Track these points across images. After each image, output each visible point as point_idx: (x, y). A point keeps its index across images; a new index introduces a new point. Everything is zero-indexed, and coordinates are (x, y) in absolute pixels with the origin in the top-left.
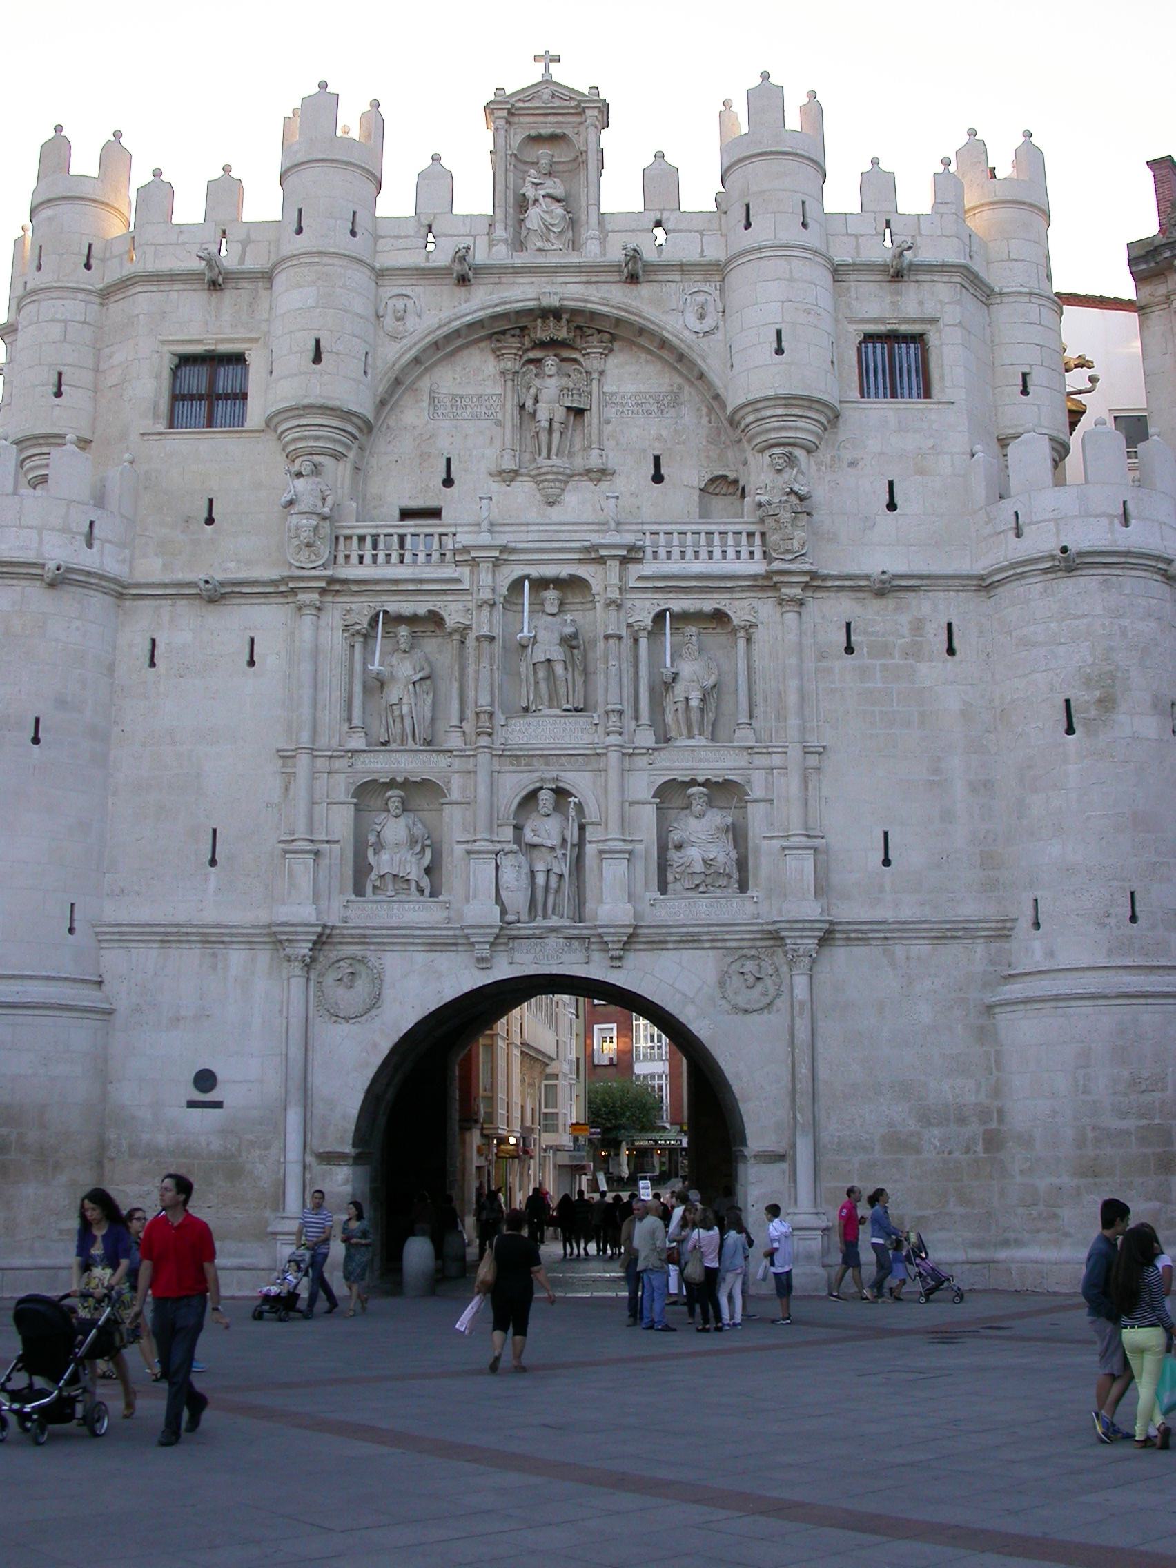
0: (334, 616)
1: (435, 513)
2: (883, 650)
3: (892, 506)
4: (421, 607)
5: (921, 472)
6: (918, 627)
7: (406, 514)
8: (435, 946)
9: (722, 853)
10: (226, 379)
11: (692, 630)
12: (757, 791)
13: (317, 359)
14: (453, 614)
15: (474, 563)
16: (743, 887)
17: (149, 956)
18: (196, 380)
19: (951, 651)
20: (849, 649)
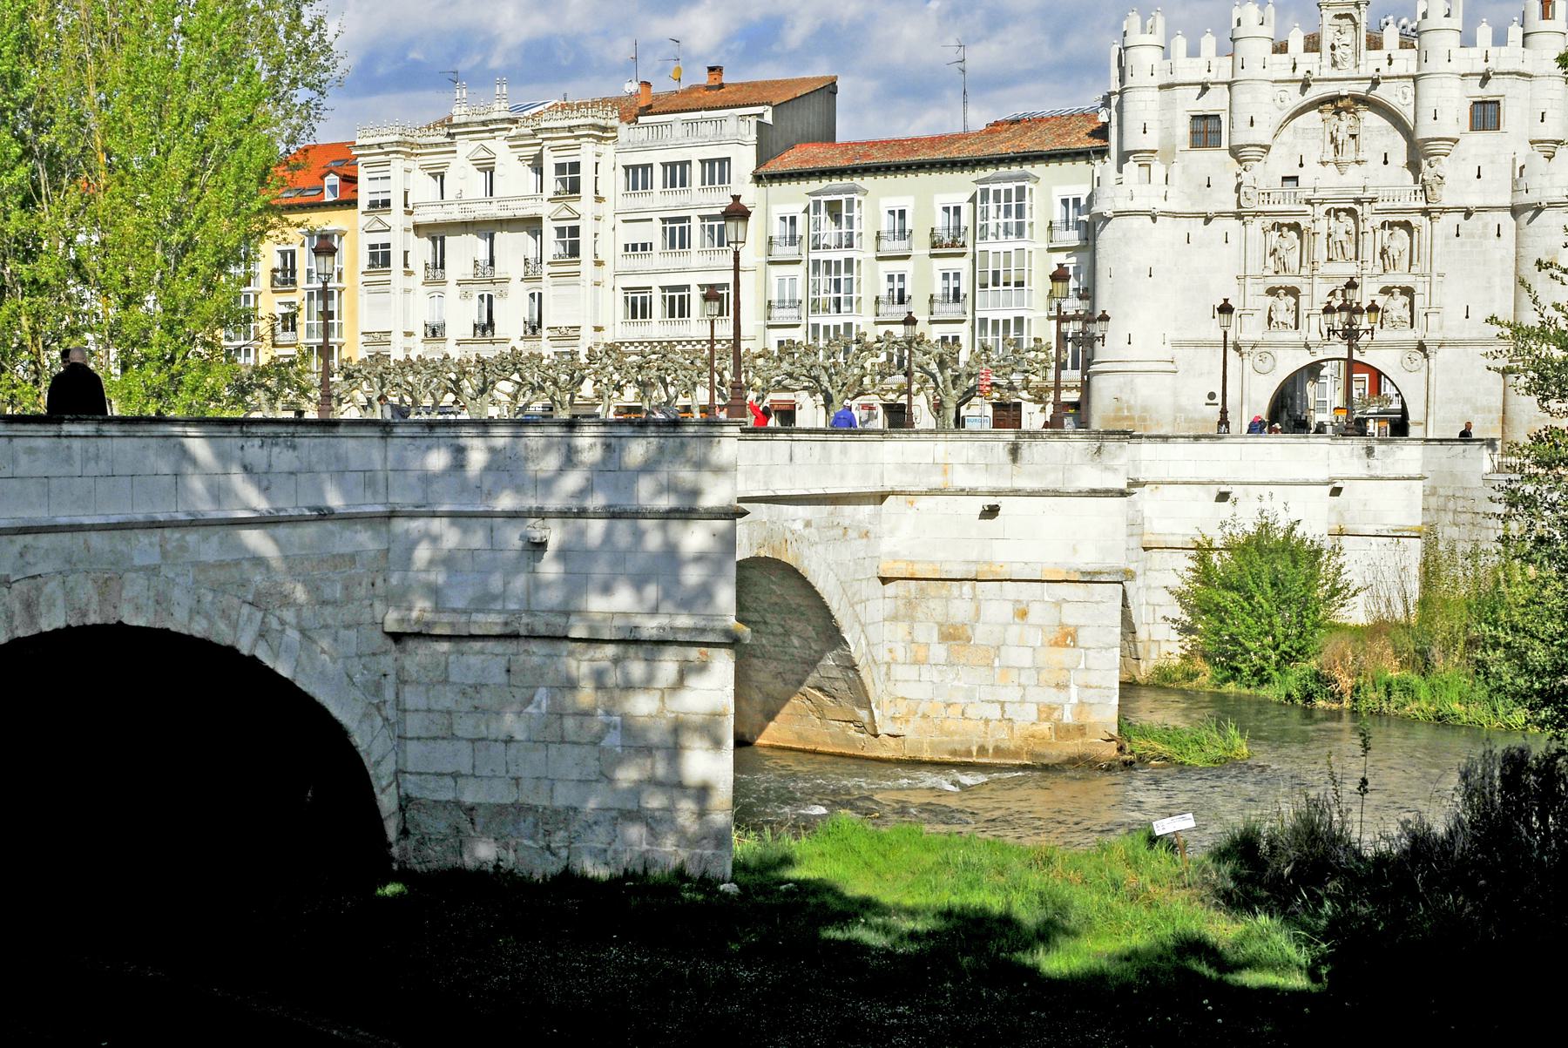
0: (1258, 222)
1: (1295, 178)
2: (1472, 235)
3: (1479, 177)
4: (1291, 220)
5: (1492, 162)
6: (1486, 226)
7: (1285, 179)
8: (1296, 347)
9: (1406, 314)
10: (1211, 125)
11: (1396, 228)
12: (1418, 290)
13: (1252, 123)
14: (1304, 222)
15: (1312, 204)
16: (1412, 326)
17: (1189, 352)
18: (1201, 125)
19: (1499, 235)
20: (1458, 235)
